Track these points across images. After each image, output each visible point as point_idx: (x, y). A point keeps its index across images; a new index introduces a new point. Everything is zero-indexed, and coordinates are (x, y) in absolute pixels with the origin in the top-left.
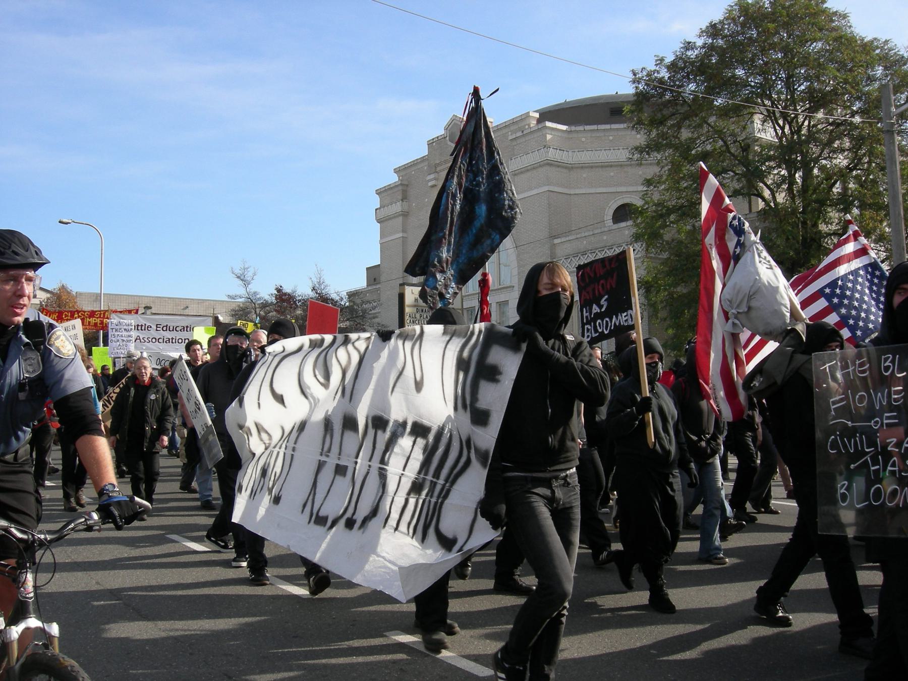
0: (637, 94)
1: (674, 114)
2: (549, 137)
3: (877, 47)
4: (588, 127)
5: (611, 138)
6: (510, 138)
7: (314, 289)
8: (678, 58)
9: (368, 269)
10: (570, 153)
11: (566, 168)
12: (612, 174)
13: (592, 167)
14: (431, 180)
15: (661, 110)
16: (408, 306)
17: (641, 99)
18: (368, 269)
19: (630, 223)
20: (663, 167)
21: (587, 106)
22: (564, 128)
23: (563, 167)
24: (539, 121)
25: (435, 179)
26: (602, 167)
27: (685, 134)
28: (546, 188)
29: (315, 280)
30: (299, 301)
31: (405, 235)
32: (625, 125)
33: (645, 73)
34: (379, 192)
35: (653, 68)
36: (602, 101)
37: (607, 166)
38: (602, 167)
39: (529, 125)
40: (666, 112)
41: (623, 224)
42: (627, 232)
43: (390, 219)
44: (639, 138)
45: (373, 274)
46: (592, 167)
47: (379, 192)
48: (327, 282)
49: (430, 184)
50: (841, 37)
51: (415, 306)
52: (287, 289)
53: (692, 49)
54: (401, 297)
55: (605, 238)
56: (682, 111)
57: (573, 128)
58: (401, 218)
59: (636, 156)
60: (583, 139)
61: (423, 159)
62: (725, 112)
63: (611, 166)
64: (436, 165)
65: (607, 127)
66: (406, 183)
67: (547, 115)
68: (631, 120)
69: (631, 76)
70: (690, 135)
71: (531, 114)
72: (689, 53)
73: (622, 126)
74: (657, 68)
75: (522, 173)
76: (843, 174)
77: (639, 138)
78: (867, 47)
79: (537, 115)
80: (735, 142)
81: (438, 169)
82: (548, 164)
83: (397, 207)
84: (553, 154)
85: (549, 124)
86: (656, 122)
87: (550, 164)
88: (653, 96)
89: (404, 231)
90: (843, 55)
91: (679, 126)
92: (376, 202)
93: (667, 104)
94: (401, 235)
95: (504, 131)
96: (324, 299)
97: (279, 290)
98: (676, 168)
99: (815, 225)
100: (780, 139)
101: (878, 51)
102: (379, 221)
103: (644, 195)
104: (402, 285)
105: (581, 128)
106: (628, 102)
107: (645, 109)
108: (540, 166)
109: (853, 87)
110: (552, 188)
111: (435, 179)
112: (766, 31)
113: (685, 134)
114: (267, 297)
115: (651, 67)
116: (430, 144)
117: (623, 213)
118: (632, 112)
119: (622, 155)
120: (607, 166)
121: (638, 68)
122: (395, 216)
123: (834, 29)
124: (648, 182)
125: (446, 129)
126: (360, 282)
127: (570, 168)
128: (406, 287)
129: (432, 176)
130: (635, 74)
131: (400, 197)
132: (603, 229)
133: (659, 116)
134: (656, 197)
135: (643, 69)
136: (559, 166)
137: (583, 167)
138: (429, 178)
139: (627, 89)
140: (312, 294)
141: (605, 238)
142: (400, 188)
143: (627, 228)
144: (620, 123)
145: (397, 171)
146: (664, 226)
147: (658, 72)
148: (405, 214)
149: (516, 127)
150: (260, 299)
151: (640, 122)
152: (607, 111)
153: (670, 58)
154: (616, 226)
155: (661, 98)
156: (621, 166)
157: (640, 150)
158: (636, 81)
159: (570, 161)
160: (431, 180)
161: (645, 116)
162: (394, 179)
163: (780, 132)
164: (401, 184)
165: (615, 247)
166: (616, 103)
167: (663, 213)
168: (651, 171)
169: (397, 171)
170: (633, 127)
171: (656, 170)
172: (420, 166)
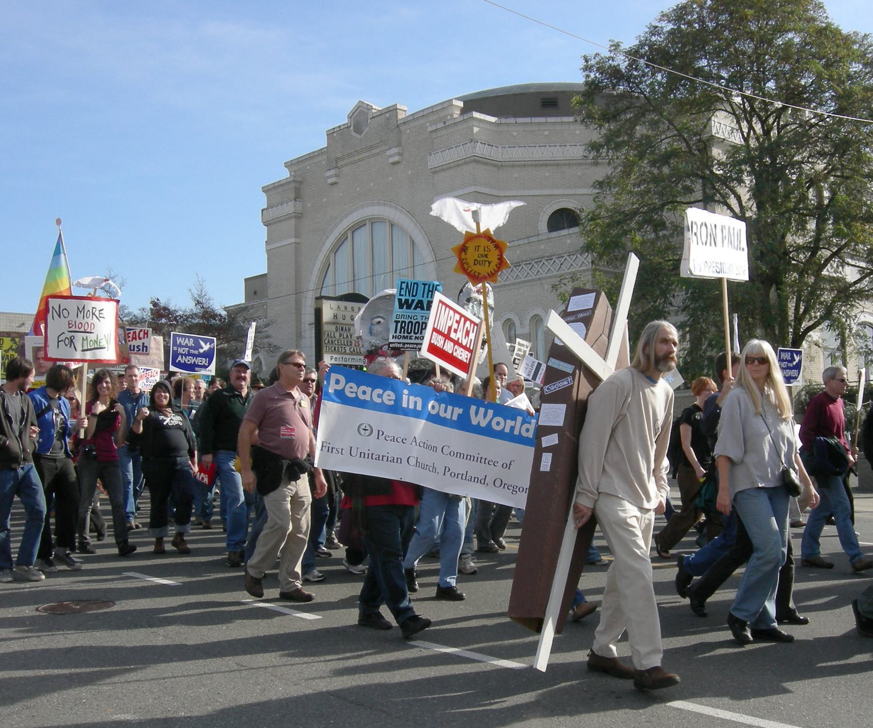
0: (587, 83)
1: (628, 108)
2: (476, 130)
3: (855, 42)
4: (520, 120)
5: (546, 133)
6: (430, 129)
7: (198, 303)
8: (642, 45)
9: (246, 280)
10: (500, 149)
11: (495, 166)
12: (547, 174)
13: (524, 166)
14: (330, 177)
15: (616, 103)
16: (327, 323)
17: (592, 89)
18: (246, 280)
19: (576, 230)
20: (615, 168)
21: (514, 95)
22: (493, 119)
23: (491, 165)
24: (464, 111)
25: (337, 176)
26: (536, 165)
27: (640, 130)
28: (473, 189)
29: (196, 293)
30: (181, 317)
31: (298, 240)
32: (571, 119)
33: (597, 59)
34: (266, 190)
35: (608, 55)
36: (531, 90)
37: (542, 165)
38: (536, 165)
39: (452, 115)
40: (620, 105)
41: (564, 232)
42: (569, 241)
43: (280, 221)
44: (595, 134)
45: (255, 287)
46: (524, 165)
47: (266, 190)
48: (210, 294)
49: (330, 181)
50: (825, 29)
51: (334, 323)
52: (162, 303)
53: (659, 34)
54: (318, 313)
55: (542, 247)
56: (638, 105)
57: (503, 120)
58: (293, 221)
59: (593, 154)
60: (515, 134)
61: (321, 152)
62: (682, 107)
63: (546, 165)
64: (337, 160)
65: (542, 120)
66: (299, 179)
67: (473, 103)
68: (580, 113)
69: (582, 63)
70: (644, 132)
71: (455, 103)
72: (653, 39)
73: (565, 119)
74: (612, 55)
75: (443, 170)
76: (814, 181)
77: (595, 134)
78: (847, 41)
79: (461, 104)
80: (700, 140)
81: (339, 164)
82: (475, 161)
83: (289, 208)
84: (480, 150)
85: (476, 115)
86: (606, 117)
87: (477, 160)
88: (606, 87)
89: (296, 237)
90: (830, 50)
91: (634, 122)
92: (263, 201)
93: (621, 96)
94: (293, 240)
95: (421, 122)
96: (208, 314)
97: (155, 304)
98: (628, 168)
99: (783, 237)
100: (746, 139)
101: (856, 47)
102: (266, 224)
103: (596, 198)
104: (319, 298)
105: (512, 120)
106: (578, 93)
107: (597, 99)
108: (466, 163)
109: (838, 85)
110: (479, 189)
111: (337, 176)
112: (743, 19)
113: (640, 130)
114: (137, 312)
115: (605, 53)
116: (330, 134)
117: (563, 219)
118: (581, 103)
119: (578, 152)
120: (542, 165)
121: (591, 53)
122: (287, 218)
123: (813, 19)
124: (600, 184)
125: (350, 117)
126: (237, 297)
127: (499, 166)
128: (324, 301)
129: (332, 172)
130: (587, 61)
131: (292, 196)
132: (540, 238)
133: (613, 109)
134: (609, 201)
135: (597, 54)
136: (486, 164)
137: (513, 165)
138: (328, 174)
139: (575, 77)
140: (197, 310)
141: (542, 247)
142: (293, 185)
143: (571, 237)
144: (557, 116)
145: (288, 165)
146: (625, 233)
147: (613, 59)
148: (298, 217)
149: (435, 117)
150: (129, 314)
151: (590, 116)
152: (547, 102)
153: (629, 42)
154: (555, 234)
155: (614, 89)
156: (558, 165)
157: (595, 147)
158: (587, 68)
159: (500, 158)
160: (330, 177)
161: (596, 109)
162: (285, 174)
163: (746, 130)
164: (294, 181)
165: (554, 258)
166: (548, 93)
167: (621, 219)
168: (601, 173)
169: (289, 165)
170: (583, 121)
171: (609, 170)
172: (316, 160)
